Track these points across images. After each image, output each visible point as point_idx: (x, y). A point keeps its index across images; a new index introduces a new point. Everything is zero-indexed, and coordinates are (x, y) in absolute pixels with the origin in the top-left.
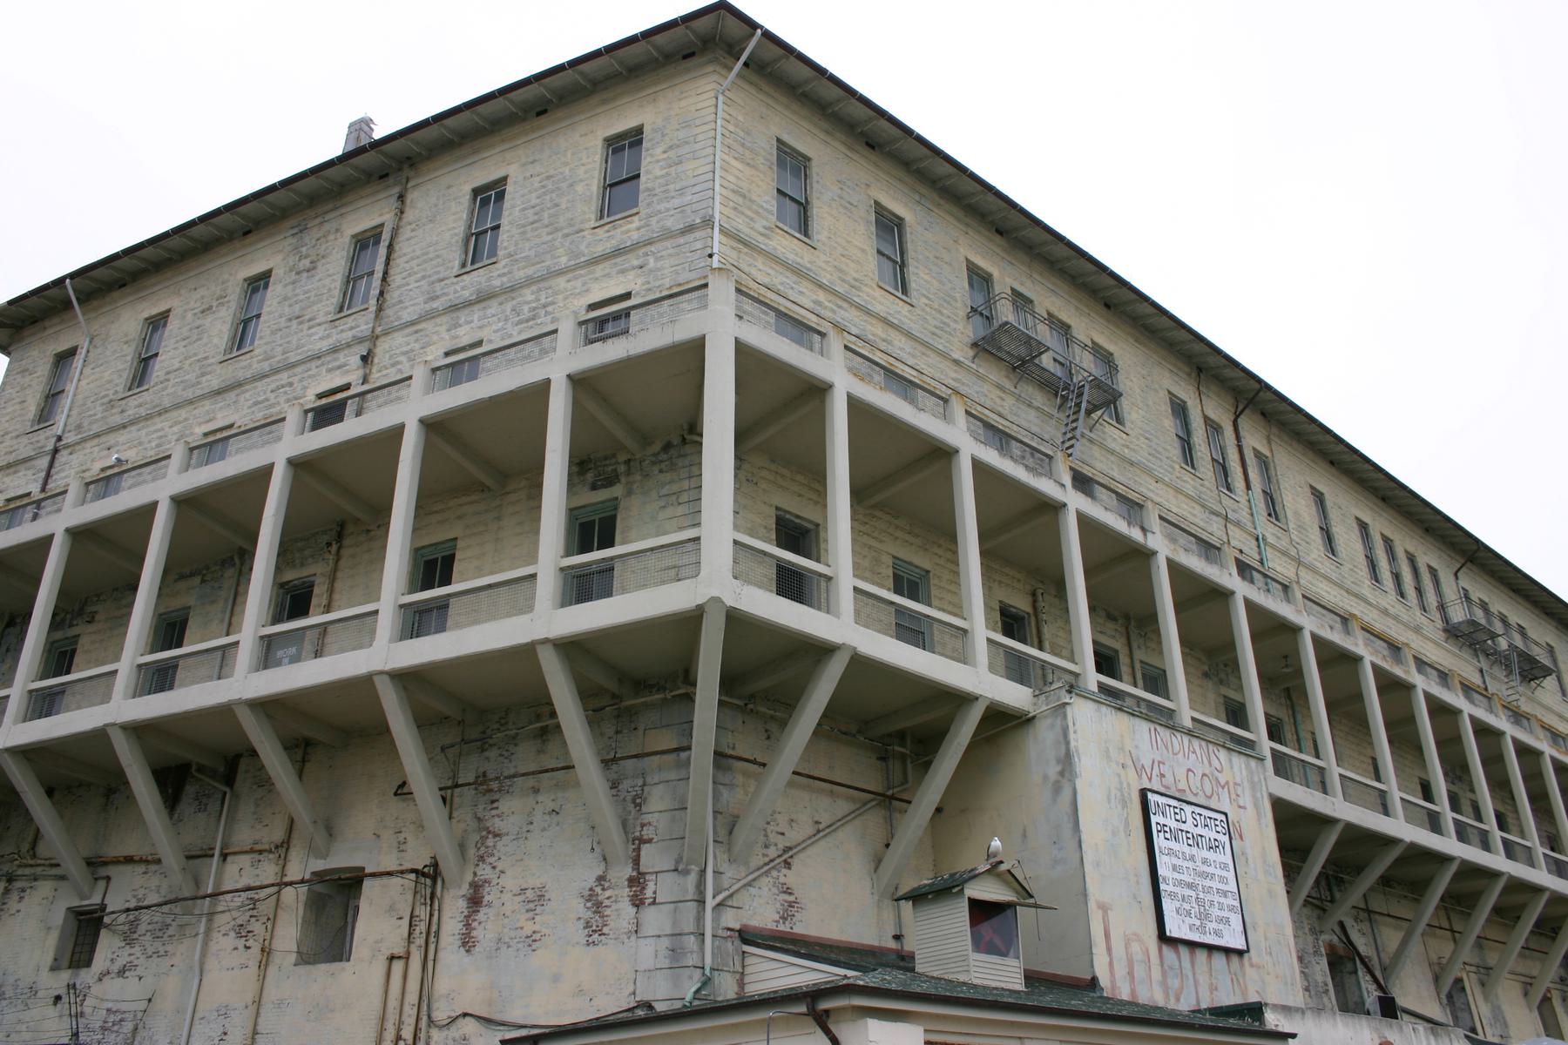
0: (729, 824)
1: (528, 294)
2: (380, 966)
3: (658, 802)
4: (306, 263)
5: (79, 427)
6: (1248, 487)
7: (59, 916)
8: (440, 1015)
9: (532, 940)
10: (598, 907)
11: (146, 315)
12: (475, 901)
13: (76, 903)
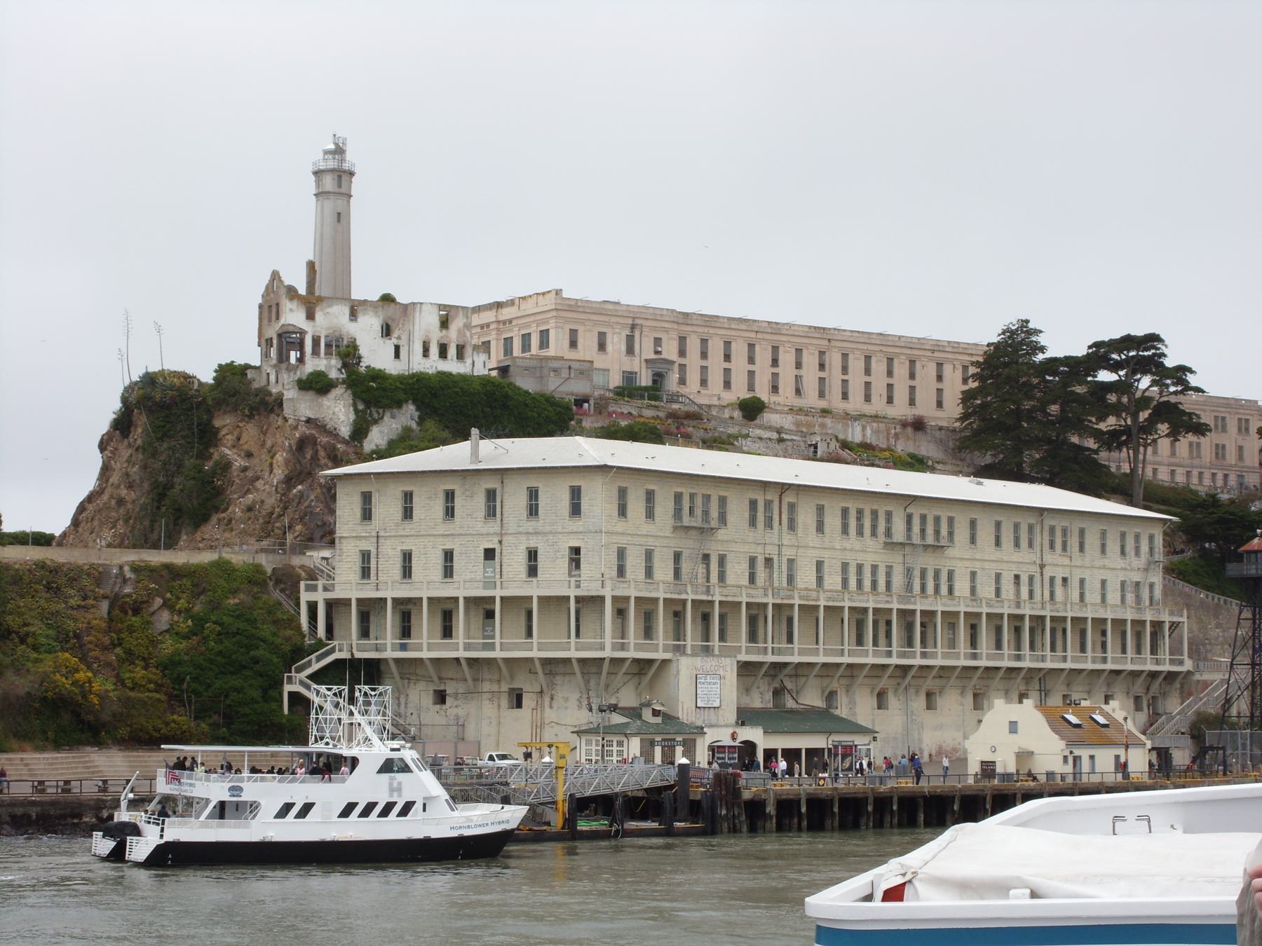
0: (607, 686)
1: (551, 537)
2: (530, 711)
3: (592, 683)
4: (468, 493)
5: (385, 529)
6: (780, 524)
7: (431, 692)
8: (547, 722)
9: (566, 708)
10: (580, 702)
11: (402, 489)
12: (552, 699)
13: (436, 688)
